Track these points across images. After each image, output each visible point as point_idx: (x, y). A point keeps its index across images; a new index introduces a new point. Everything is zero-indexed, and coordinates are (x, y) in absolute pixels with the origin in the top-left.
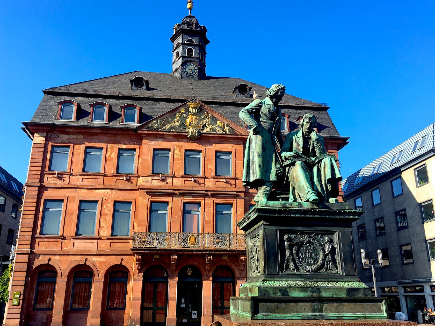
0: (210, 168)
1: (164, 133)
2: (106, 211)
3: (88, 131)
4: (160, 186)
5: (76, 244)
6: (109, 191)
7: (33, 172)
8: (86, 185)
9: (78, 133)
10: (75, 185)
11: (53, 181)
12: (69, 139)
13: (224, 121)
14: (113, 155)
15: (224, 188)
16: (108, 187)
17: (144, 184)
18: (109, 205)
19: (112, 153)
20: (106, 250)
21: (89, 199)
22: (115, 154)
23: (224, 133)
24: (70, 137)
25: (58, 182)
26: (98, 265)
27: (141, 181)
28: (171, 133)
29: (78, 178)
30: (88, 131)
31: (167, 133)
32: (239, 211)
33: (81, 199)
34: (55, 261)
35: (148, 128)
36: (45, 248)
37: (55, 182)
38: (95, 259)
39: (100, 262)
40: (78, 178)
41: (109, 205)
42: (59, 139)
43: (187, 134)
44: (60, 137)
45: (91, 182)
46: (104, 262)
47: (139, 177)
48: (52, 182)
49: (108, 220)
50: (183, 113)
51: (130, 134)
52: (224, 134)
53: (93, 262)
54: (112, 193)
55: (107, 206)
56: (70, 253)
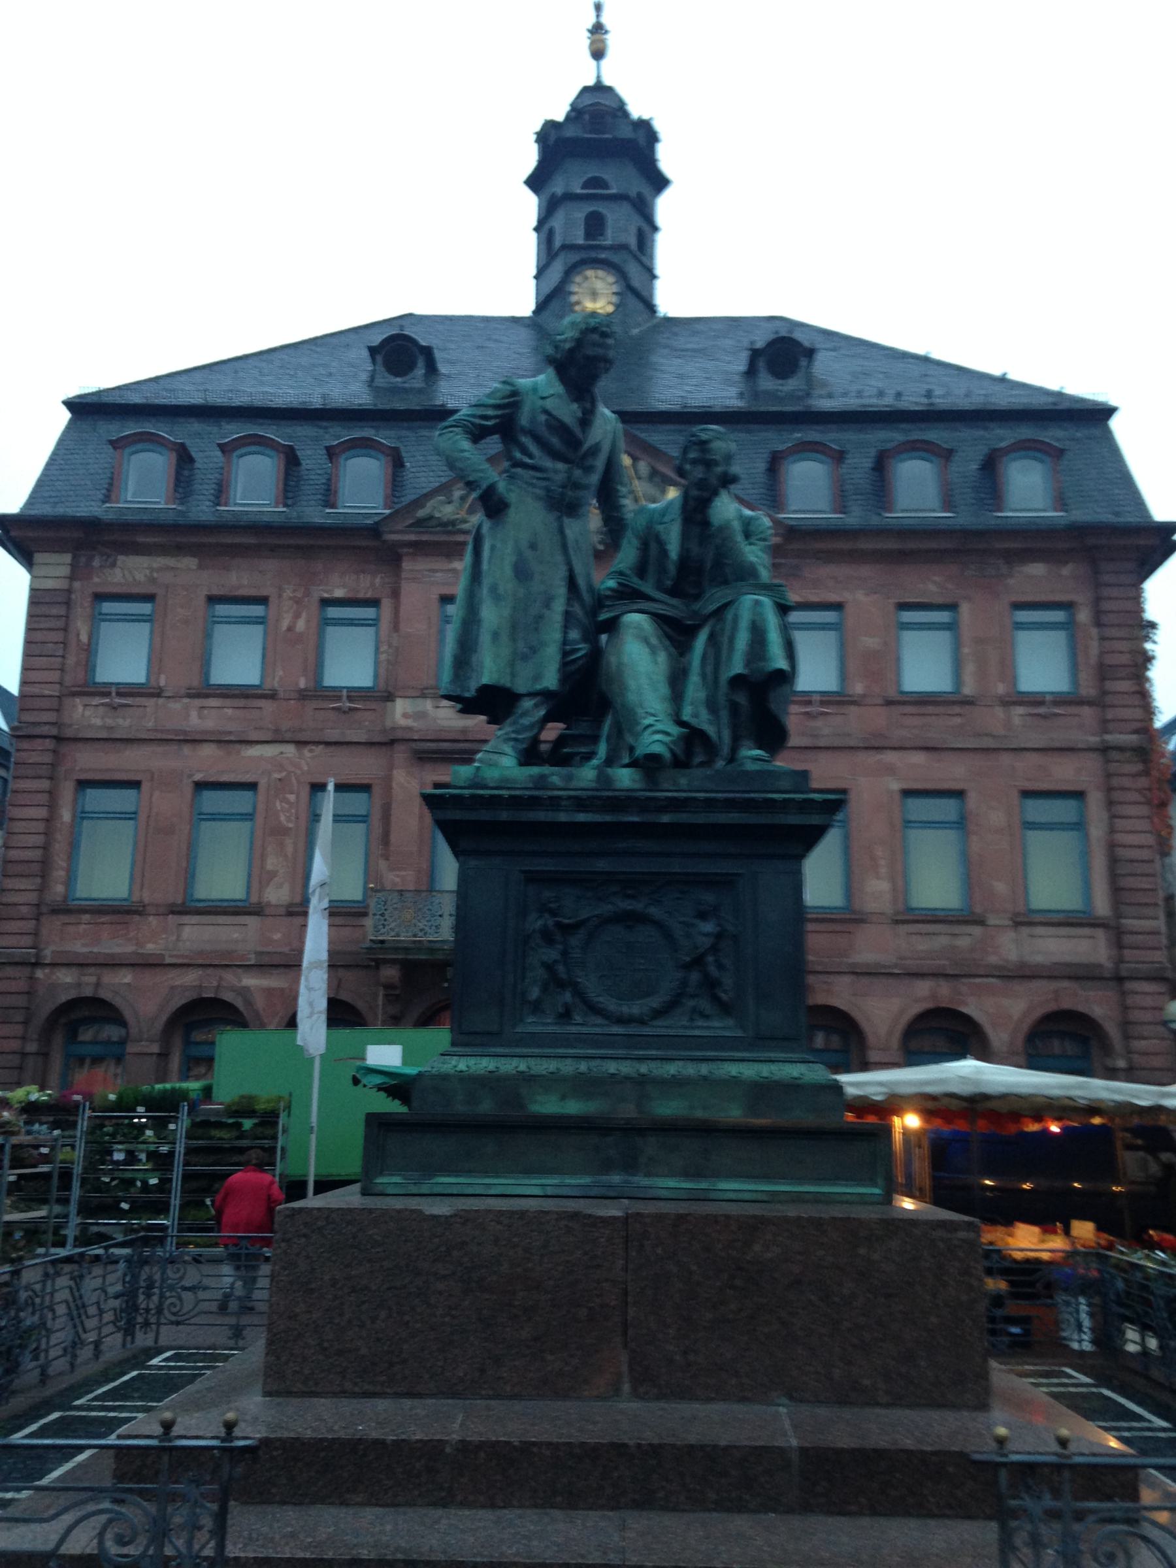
2: (283, 818)
3: (212, 540)
4: (464, 731)
5: (187, 932)
6: (290, 750)
7: (35, 690)
9: (179, 550)
10: (177, 732)
11: (102, 718)
12: (152, 570)
14: (301, 625)
16: (288, 736)
17: (409, 722)
18: (292, 798)
19: (297, 616)
20: (286, 950)
21: (225, 778)
22: (308, 621)
24: (155, 565)
25: (120, 721)
26: (260, 1003)
27: (401, 711)
30: (212, 540)
33: (198, 777)
34: (118, 984)
35: (420, 523)
36: (84, 945)
37: (109, 722)
38: (251, 981)
39: (269, 992)
41: (292, 798)
42: (117, 571)
44: (119, 563)
46: (282, 990)
47: (389, 697)
48: (99, 722)
49: (290, 849)
51: (359, 548)
53: (244, 992)
55: (288, 802)
56: (168, 961)
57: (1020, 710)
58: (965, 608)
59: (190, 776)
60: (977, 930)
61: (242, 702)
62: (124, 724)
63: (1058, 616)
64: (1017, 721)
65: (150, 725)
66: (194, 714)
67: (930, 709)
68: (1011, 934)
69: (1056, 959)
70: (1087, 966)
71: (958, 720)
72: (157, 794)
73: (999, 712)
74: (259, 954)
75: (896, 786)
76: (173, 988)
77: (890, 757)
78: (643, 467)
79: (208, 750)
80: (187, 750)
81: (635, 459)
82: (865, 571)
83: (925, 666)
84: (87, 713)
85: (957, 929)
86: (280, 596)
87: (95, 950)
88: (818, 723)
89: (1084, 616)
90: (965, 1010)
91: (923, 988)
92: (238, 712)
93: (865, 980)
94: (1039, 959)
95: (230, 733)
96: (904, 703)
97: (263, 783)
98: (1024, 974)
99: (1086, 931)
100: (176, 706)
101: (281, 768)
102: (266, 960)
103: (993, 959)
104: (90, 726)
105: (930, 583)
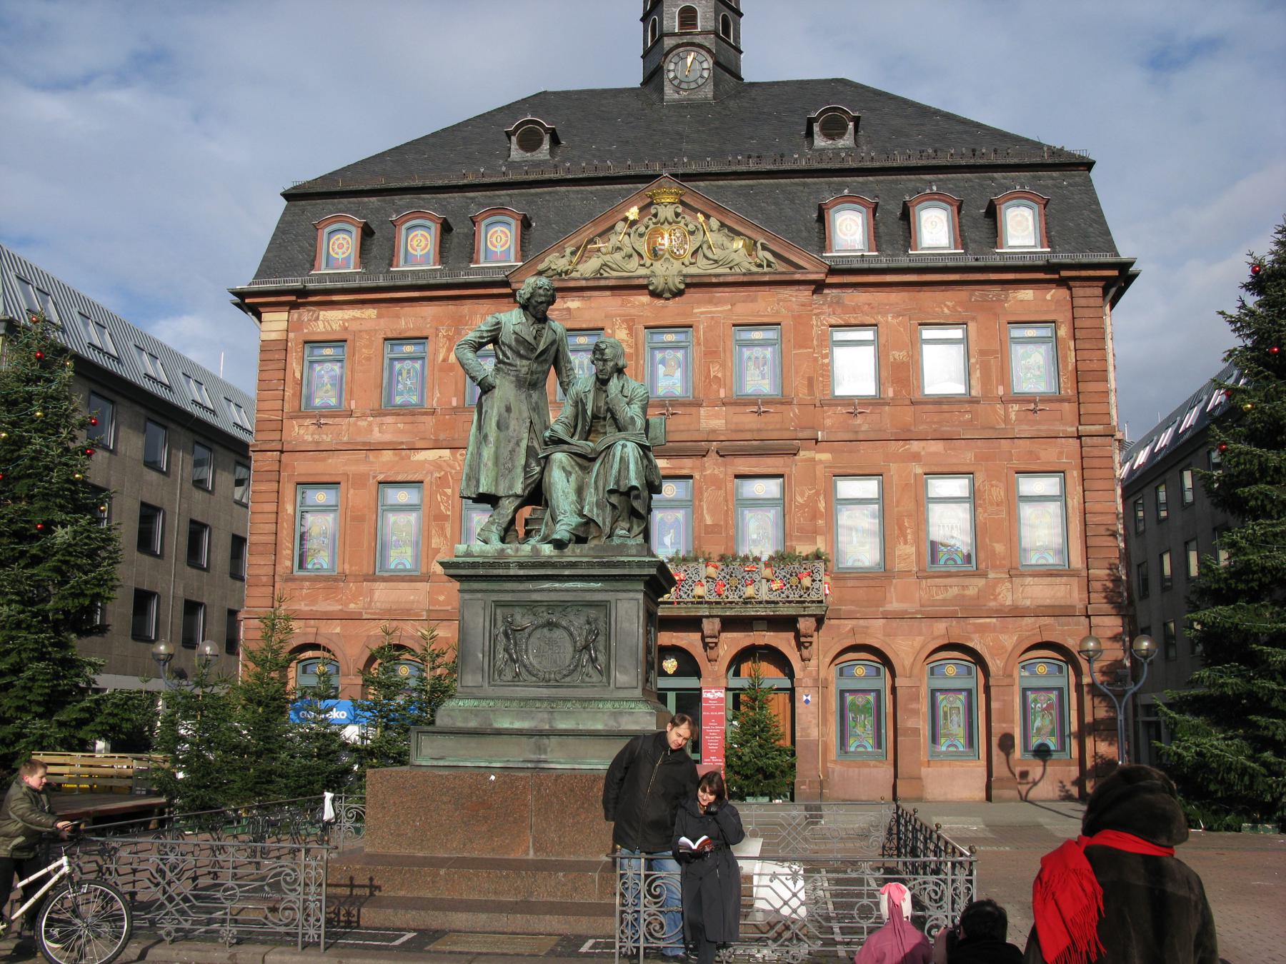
0: (715, 377)
1: (583, 283)
6: (446, 453)
8: (390, 443)
13: (753, 235)
15: (759, 430)
23: (755, 269)
28: (603, 283)
29: (370, 424)
31: (591, 283)
32: (802, 495)
33: (381, 478)
37: (316, 437)
40: (370, 424)
42: (320, 323)
43: (645, 282)
45: (402, 432)
50: (634, 223)
52: (757, 273)
54: (455, 459)
57: (1016, 407)
58: (972, 326)
59: (375, 477)
60: (981, 582)
61: (409, 419)
62: (327, 438)
63: (1046, 332)
64: (1013, 416)
65: (345, 439)
66: (376, 429)
67: (945, 407)
68: (1008, 584)
69: (1040, 602)
70: (1061, 606)
71: (968, 416)
72: (351, 491)
73: (999, 408)
74: (429, 611)
75: (919, 470)
76: (368, 636)
77: (915, 446)
78: (714, 223)
79: (387, 456)
80: (371, 455)
81: (707, 217)
82: (895, 297)
83: (943, 368)
84: (302, 432)
85: (967, 581)
86: (437, 335)
87: (314, 608)
88: (859, 420)
89: (1063, 332)
90: (971, 644)
91: (940, 627)
92: (407, 427)
93: (895, 623)
94: (1028, 603)
95: (402, 443)
96: (926, 403)
97: (427, 480)
98: (1017, 613)
99: (1064, 579)
100: (363, 424)
101: (439, 468)
102: (434, 616)
103: (992, 604)
104: (305, 442)
105: (946, 302)
